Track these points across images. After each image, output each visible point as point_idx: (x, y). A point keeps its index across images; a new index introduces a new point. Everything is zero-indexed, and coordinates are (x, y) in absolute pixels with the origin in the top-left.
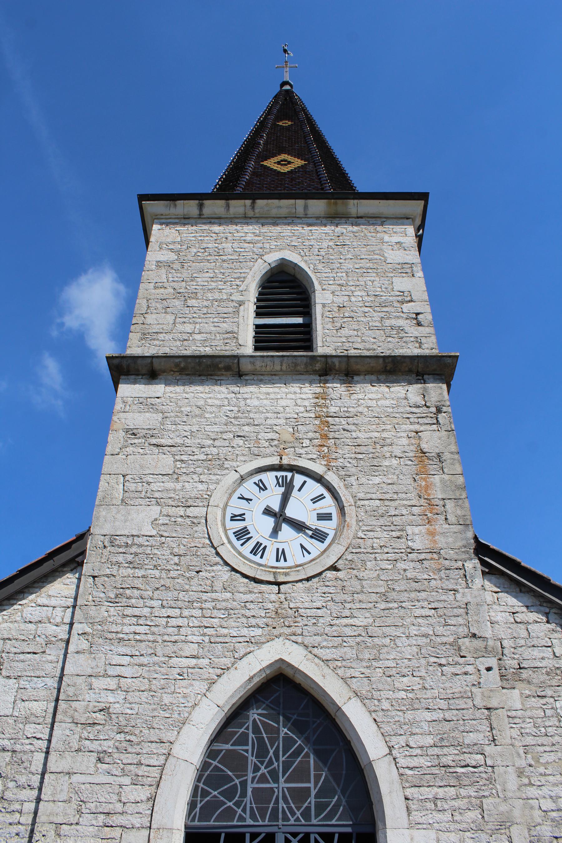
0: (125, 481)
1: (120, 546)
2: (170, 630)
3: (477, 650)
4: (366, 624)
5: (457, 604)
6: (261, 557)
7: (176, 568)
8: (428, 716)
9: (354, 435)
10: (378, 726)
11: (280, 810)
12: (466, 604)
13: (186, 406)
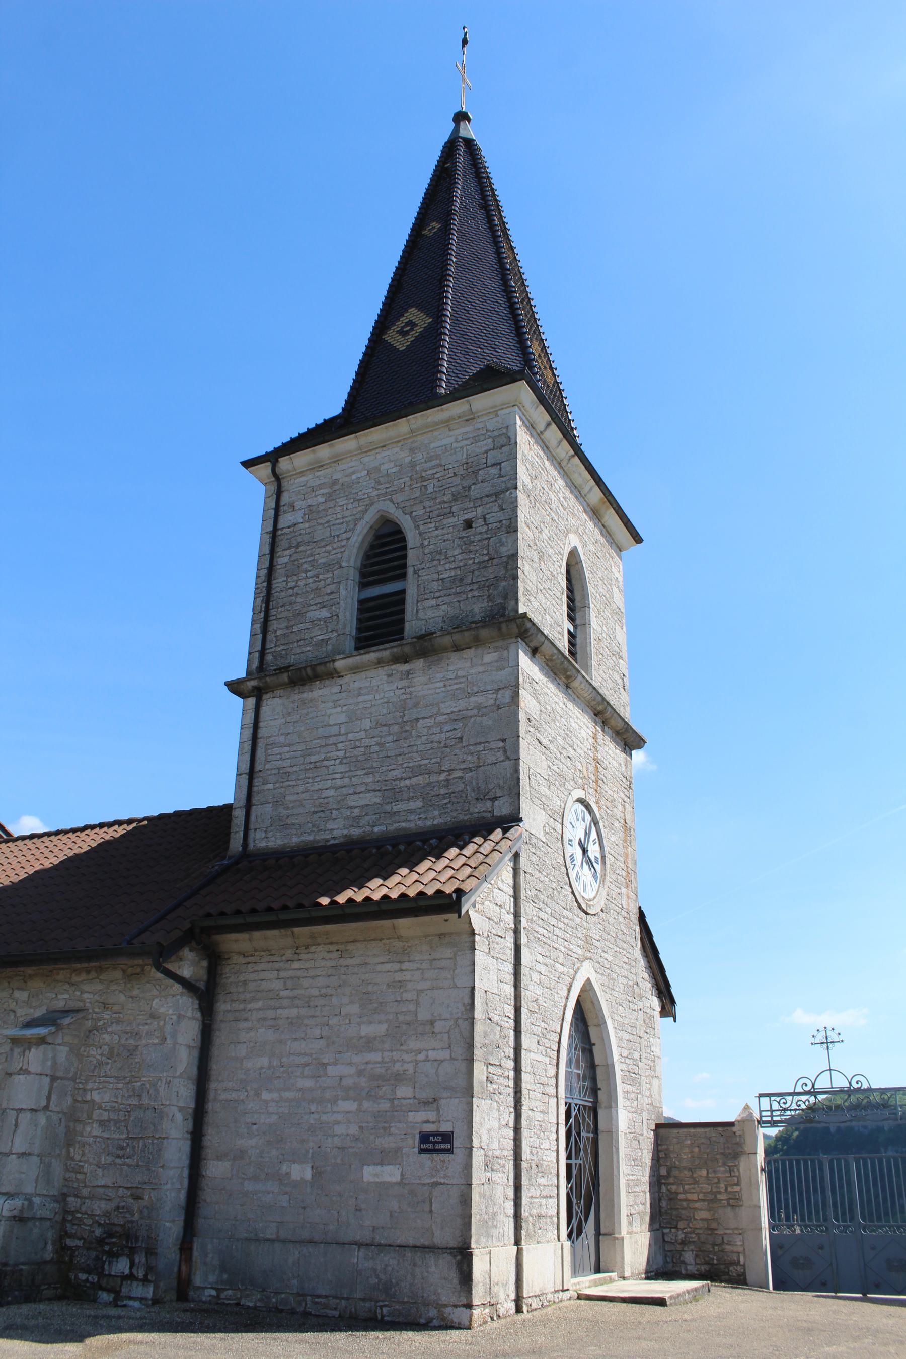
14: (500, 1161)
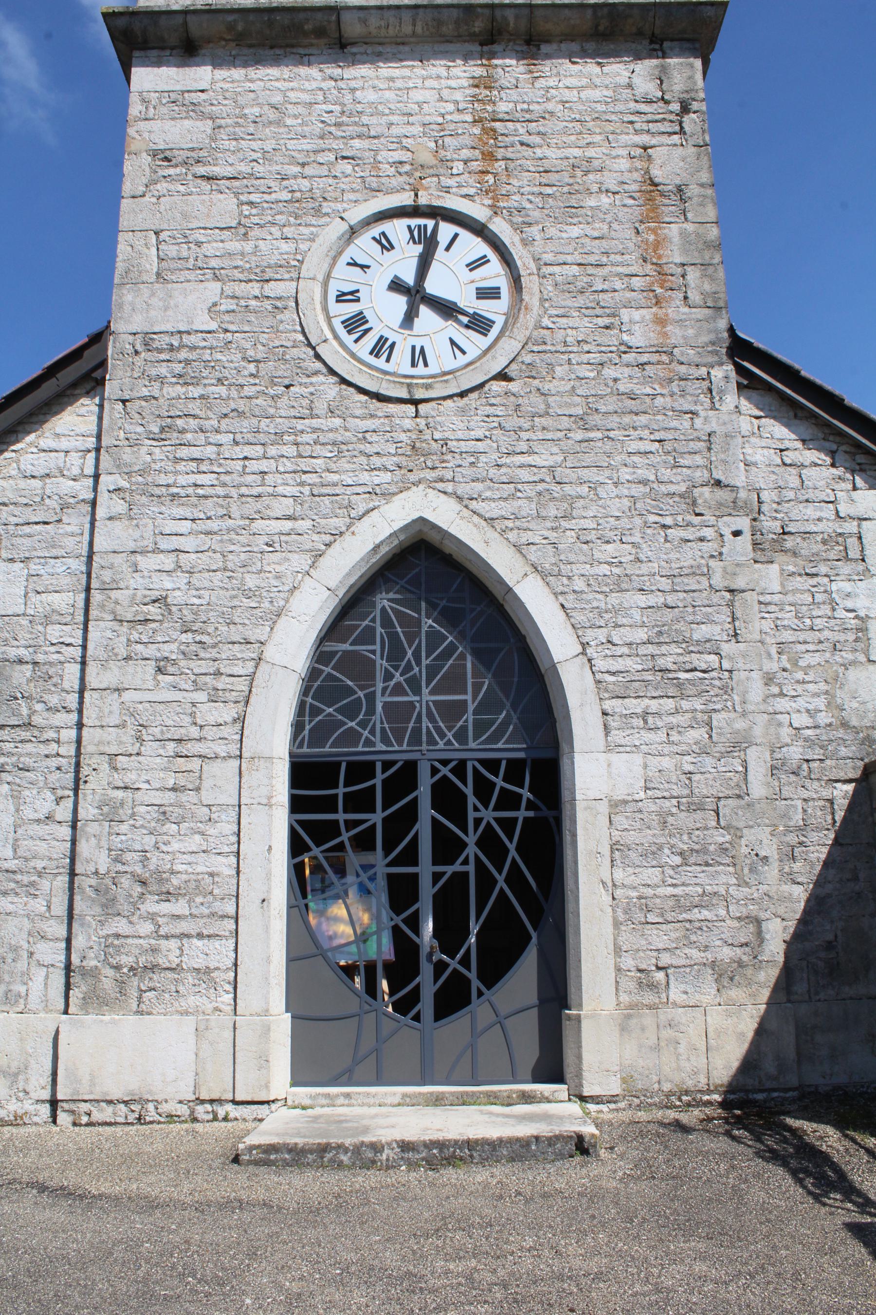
0: (158, 243)
1: (160, 351)
2: (249, 479)
3: (721, 504)
4: (552, 464)
5: (695, 434)
6: (388, 360)
7: (252, 381)
8: (642, 600)
9: (539, 152)
10: (567, 614)
11: (424, 731)
12: (709, 435)
13: (252, 106)
14: (19, 877)
